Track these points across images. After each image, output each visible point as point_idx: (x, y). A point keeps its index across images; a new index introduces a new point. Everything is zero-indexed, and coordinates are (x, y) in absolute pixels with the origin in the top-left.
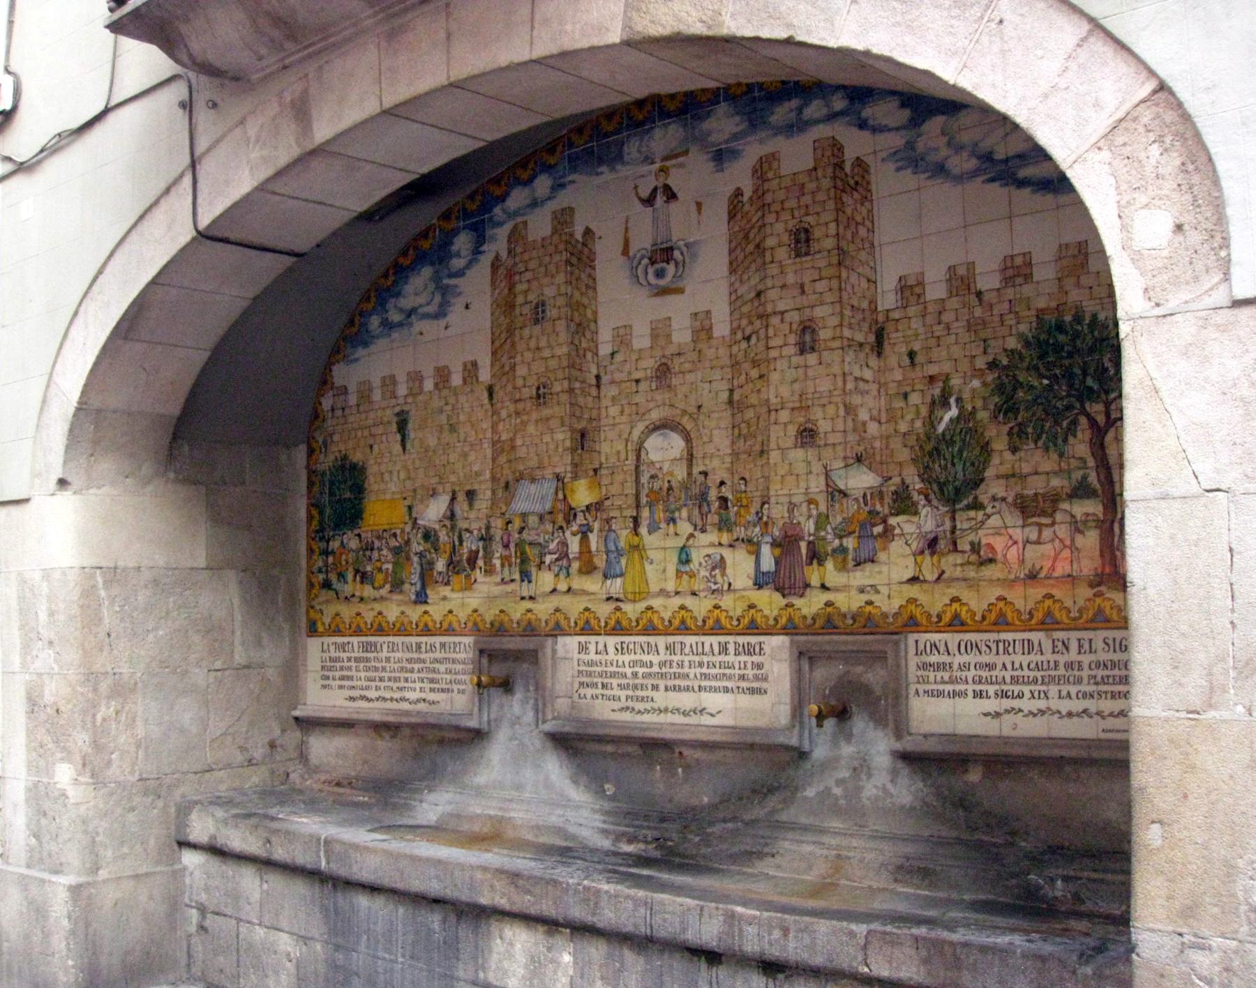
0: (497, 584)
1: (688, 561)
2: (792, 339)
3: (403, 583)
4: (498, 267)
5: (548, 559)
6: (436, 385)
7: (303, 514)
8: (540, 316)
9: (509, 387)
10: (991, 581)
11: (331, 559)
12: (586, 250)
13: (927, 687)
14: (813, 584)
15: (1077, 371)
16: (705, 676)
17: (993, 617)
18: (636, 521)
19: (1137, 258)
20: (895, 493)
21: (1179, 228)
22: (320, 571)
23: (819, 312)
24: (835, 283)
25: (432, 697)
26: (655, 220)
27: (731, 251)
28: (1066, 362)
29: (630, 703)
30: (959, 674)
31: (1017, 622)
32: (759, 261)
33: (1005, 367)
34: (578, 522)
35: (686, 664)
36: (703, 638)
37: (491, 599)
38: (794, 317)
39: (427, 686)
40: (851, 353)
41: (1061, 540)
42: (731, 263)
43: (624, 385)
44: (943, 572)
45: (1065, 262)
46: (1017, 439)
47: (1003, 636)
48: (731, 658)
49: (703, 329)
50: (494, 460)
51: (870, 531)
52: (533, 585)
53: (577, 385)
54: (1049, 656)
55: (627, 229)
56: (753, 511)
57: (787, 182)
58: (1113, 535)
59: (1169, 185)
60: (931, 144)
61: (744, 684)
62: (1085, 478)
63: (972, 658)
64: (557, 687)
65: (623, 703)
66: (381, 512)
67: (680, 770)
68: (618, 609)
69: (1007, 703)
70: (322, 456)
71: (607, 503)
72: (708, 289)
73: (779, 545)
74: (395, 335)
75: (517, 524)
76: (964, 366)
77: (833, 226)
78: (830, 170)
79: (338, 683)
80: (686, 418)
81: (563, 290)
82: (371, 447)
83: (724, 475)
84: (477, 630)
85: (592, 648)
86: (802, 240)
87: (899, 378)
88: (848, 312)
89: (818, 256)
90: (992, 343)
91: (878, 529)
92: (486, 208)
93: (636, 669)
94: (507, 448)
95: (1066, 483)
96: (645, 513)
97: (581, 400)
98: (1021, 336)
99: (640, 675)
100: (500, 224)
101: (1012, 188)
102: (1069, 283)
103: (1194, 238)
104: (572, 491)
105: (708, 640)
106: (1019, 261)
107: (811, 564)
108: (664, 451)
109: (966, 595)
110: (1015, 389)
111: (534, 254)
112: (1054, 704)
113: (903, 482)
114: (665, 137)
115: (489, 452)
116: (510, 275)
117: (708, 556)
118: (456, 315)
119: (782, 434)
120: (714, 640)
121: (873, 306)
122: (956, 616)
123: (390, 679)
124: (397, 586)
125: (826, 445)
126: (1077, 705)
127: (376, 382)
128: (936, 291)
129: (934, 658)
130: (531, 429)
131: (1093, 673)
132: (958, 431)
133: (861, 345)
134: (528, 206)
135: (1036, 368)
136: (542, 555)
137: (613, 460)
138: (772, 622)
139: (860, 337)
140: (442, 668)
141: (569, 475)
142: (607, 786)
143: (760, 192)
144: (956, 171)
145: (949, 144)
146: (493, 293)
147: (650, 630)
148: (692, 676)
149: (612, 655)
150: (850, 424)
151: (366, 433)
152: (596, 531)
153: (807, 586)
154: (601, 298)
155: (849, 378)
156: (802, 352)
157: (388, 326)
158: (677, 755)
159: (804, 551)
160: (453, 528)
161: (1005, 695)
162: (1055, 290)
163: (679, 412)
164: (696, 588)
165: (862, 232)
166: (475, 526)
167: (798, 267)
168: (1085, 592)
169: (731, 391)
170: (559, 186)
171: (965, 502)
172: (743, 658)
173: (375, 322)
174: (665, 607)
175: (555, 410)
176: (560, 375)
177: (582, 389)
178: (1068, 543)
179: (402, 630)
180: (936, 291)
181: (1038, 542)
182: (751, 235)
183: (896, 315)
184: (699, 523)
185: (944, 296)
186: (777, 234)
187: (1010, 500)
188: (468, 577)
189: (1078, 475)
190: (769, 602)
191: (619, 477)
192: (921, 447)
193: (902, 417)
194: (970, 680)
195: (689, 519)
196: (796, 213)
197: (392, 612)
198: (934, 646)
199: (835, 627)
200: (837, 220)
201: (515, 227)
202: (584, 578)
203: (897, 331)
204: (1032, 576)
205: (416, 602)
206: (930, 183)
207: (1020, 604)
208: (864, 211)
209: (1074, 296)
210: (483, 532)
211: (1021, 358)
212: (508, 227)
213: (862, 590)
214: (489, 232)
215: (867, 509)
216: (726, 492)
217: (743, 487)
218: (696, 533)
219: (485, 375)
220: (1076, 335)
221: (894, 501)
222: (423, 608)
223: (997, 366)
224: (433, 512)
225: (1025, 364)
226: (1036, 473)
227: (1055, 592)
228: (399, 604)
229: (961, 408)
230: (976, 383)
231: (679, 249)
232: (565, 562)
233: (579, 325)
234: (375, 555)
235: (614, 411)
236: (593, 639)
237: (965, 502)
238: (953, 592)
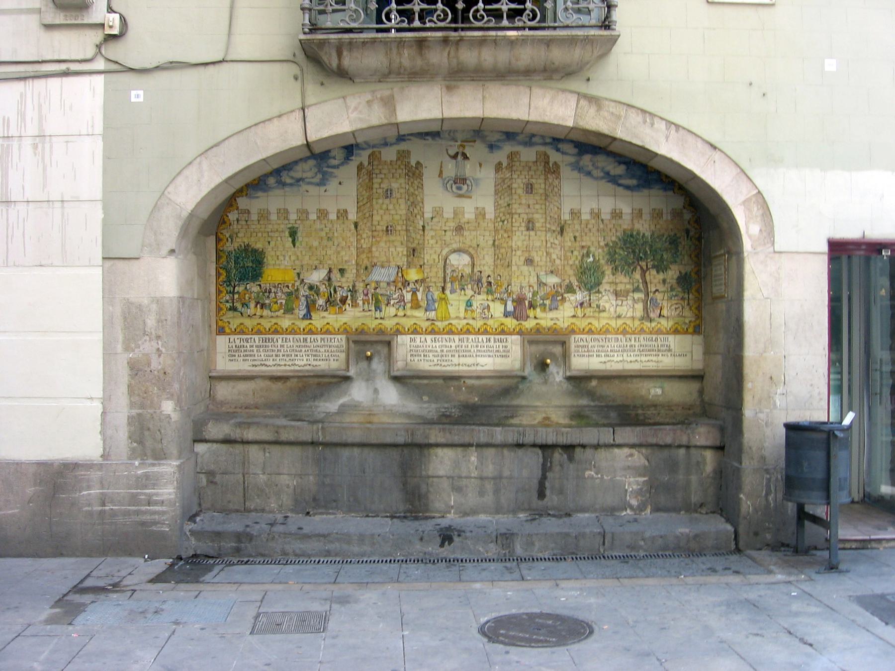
1: (471, 306)
2: (523, 224)
3: (293, 309)
5: (392, 302)
6: (318, 218)
7: (213, 272)
9: (369, 224)
11: (236, 296)
18: (443, 289)
19: (750, 237)
20: (567, 286)
21: (761, 230)
22: (227, 302)
23: (536, 216)
24: (543, 207)
25: (315, 363)
38: (525, 217)
46: (615, 270)
48: (492, 343)
49: (481, 214)
51: (556, 298)
53: (411, 228)
57: (522, 164)
59: (759, 219)
63: (596, 343)
70: (228, 244)
74: (287, 189)
75: (373, 285)
76: (596, 244)
77: (543, 186)
78: (543, 164)
79: (242, 358)
83: (490, 273)
84: (346, 332)
88: (548, 218)
96: (449, 285)
97: (413, 235)
100: (363, 149)
102: (635, 221)
103: (765, 234)
105: (480, 337)
108: (460, 261)
112: (625, 358)
115: (355, 253)
116: (370, 174)
118: (332, 185)
119: (518, 259)
120: (484, 337)
122: (590, 329)
123: (283, 355)
124: (289, 310)
126: (633, 359)
127: (273, 209)
128: (585, 217)
129: (582, 344)
130: (382, 244)
139: (554, 228)
140: (322, 350)
146: (358, 180)
147: (451, 332)
153: (528, 317)
156: (528, 229)
157: (285, 185)
160: (330, 285)
166: (345, 285)
168: (637, 323)
169: (494, 241)
172: (498, 344)
175: (398, 237)
176: (401, 222)
177: (414, 231)
179: (293, 331)
186: (518, 184)
188: (340, 308)
189: (636, 285)
190: (511, 323)
191: (434, 270)
195: (472, 289)
197: (286, 323)
201: (373, 154)
204: (619, 317)
205: (303, 319)
207: (614, 326)
212: (369, 151)
213: (552, 319)
216: (491, 280)
219: (353, 216)
228: (290, 319)
229: (594, 259)
233: (413, 203)
235: (432, 242)
236: (418, 336)
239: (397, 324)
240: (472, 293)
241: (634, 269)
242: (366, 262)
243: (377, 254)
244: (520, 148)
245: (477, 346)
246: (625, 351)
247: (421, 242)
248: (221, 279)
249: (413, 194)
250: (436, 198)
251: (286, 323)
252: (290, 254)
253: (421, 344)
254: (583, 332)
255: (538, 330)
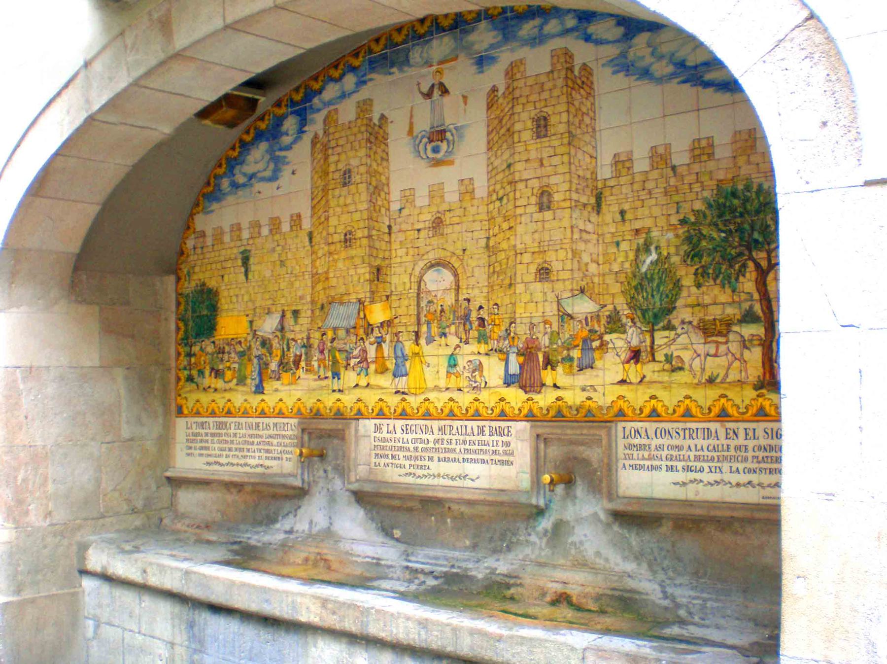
0: (315, 380)
2: (533, 200)
3: (246, 378)
4: (316, 144)
5: (353, 362)
6: (271, 230)
7: (173, 327)
8: (347, 180)
9: (324, 234)
10: (680, 384)
11: (193, 360)
12: (381, 131)
13: (632, 462)
14: (547, 384)
15: (747, 226)
16: (467, 451)
17: (681, 410)
18: (417, 334)
20: (609, 317)
22: (185, 368)
23: (553, 180)
24: (566, 159)
25: (268, 463)
26: (433, 110)
27: (489, 134)
28: (739, 220)
29: (412, 470)
30: (656, 453)
31: (700, 416)
32: (510, 141)
33: (693, 223)
34: (375, 334)
35: (454, 442)
36: (466, 423)
37: (311, 390)
38: (535, 183)
39: (264, 455)
40: (577, 211)
41: (733, 355)
42: (489, 143)
43: (408, 233)
44: (644, 377)
45: (738, 145)
46: (701, 275)
47: (689, 425)
49: (467, 190)
50: (313, 288)
52: (341, 381)
53: (374, 232)
54: (723, 441)
55: (411, 117)
56: (503, 328)
57: (530, 82)
58: (772, 352)
60: (639, 54)
61: (497, 458)
62: (751, 307)
63: (666, 441)
64: (359, 457)
65: (408, 470)
66: (231, 325)
67: (449, 520)
68: (404, 400)
69: (691, 476)
71: (396, 321)
72: (471, 161)
73: (522, 355)
74: (240, 193)
75: (330, 334)
76: (662, 222)
77: (564, 117)
78: (563, 73)
79: (198, 452)
80: (455, 258)
81: (364, 161)
82: (223, 276)
85: (385, 429)
86: (542, 126)
87: (613, 230)
88: (575, 181)
89: (553, 138)
90: (683, 205)
91: (596, 344)
92: (308, 98)
93: (416, 445)
94: (322, 278)
95: (736, 311)
96: (424, 328)
98: (704, 199)
99: (420, 449)
100: (319, 110)
101: (700, 88)
102: (741, 160)
104: (371, 312)
106: (704, 143)
107: (546, 369)
108: (438, 282)
109: (661, 394)
110: (699, 241)
111: (343, 134)
112: (727, 477)
113: (615, 308)
114: (441, 46)
116: (326, 147)
117: (470, 361)
120: (475, 424)
121: (594, 176)
123: (236, 450)
124: (241, 381)
125: (558, 280)
126: (743, 478)
129: (637, 441)
130: (340, 265)
131: (757, 454)
132: (656, 271)
133: (585, 205)
134: (340, 97)
135: (716, 225)
136: (348, 359)
137: (400, 288)
138: (517, 412)
139: (584, 199)
140: (275, 441)
141: (368, 300)
142: (395, 531)
143: (511, 90)
144: (657, 74)
145: (653, 54)
147: (427, 416)
148: (458, 451)
149: (399, 435)
150: (576, 266)
151: (219, 266)
152: (387, 342)
153: (543, 385)
154: (392, 168)
155: (575, 230)
157: (235, 186)
158: (446, 509)
159: (541, 359)
161: (689, 469)
162: (731, 165)
163: (449, 254)
164: (461, 385)
165: (587, 120)
167: (539, 146)
168: (750, 393)
170: (361, 83)
171: (661, 324)
172: (495, 438)
173: (225, 183)
174: (439, 400)
175: (359, 251)
178: (738, 356)
179: (246, 414)
180: (641, 165)
181: (716, 355)
182: (504, 122)
183: (612, 183)
184: (464, 337)
185: (647, 169)
187: (695, 323)
189: (746, 306)
190: (515, 397)
191: (405, 302)
192: (628, 282)
193: (615, 260)
194: (664, 458)
195: (457, 334)
196: (538, 105)
198: (637, 432)
199: (563, 416)
200: (568, 111)
201: (330, 112)
202: (379, 376)
203: (612, 195)
204: (711, 381)
205: (255, 393)
206: (639, 83)
207: (701, 402)
208: (589, 104)
209: (745, 171)
210: (305, 341)
211: (705, 216)
212: (324, 112)
214: (310, 117)
215: (588, 328)
216: (484, 314)
217: (496, 310)
218: (461, 345)
220: (746, 200)
221: (608, 323)
222: (261, 397)
223: (686, 222)
224: (268, 326)
225: (707, 222)
226: (715, 304)
227: (728, 393)
229: (660, 254)
230: (670, 235)
231: (450, 131)
232: (364, 365)
233: (376, 187)
234: (226, 357)
237: (661, 324)
238: (652, 392)
239: (359, 400)
240: (456, 341)
241: (741, 272)
242: (322, 298)
243: (333, 282)
244: (524, 52)
245: (464, 442)
246: (725, 458)
247: (387, 254)
248: (180, 336)
249: (376, 171)
250: (408, 173)
251: (239, 398)
252: (243, 292)
253: (389, 436)
254: (639, 415)
255: (559, 413)
